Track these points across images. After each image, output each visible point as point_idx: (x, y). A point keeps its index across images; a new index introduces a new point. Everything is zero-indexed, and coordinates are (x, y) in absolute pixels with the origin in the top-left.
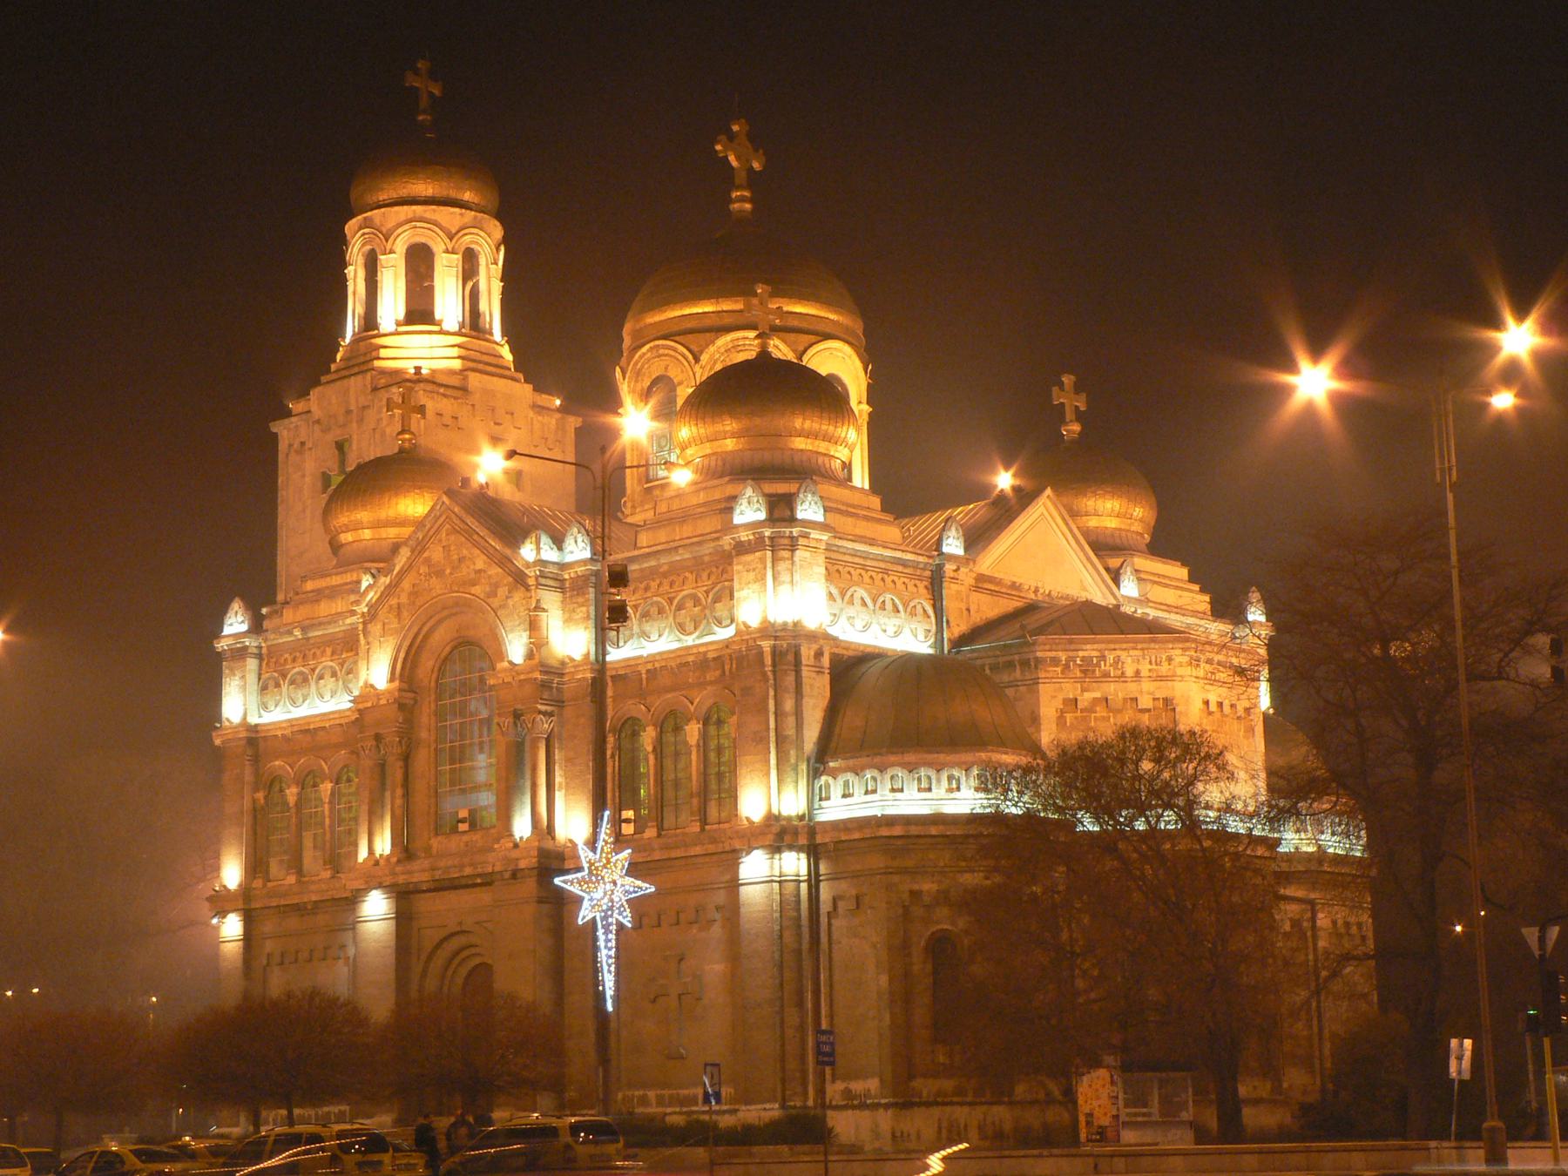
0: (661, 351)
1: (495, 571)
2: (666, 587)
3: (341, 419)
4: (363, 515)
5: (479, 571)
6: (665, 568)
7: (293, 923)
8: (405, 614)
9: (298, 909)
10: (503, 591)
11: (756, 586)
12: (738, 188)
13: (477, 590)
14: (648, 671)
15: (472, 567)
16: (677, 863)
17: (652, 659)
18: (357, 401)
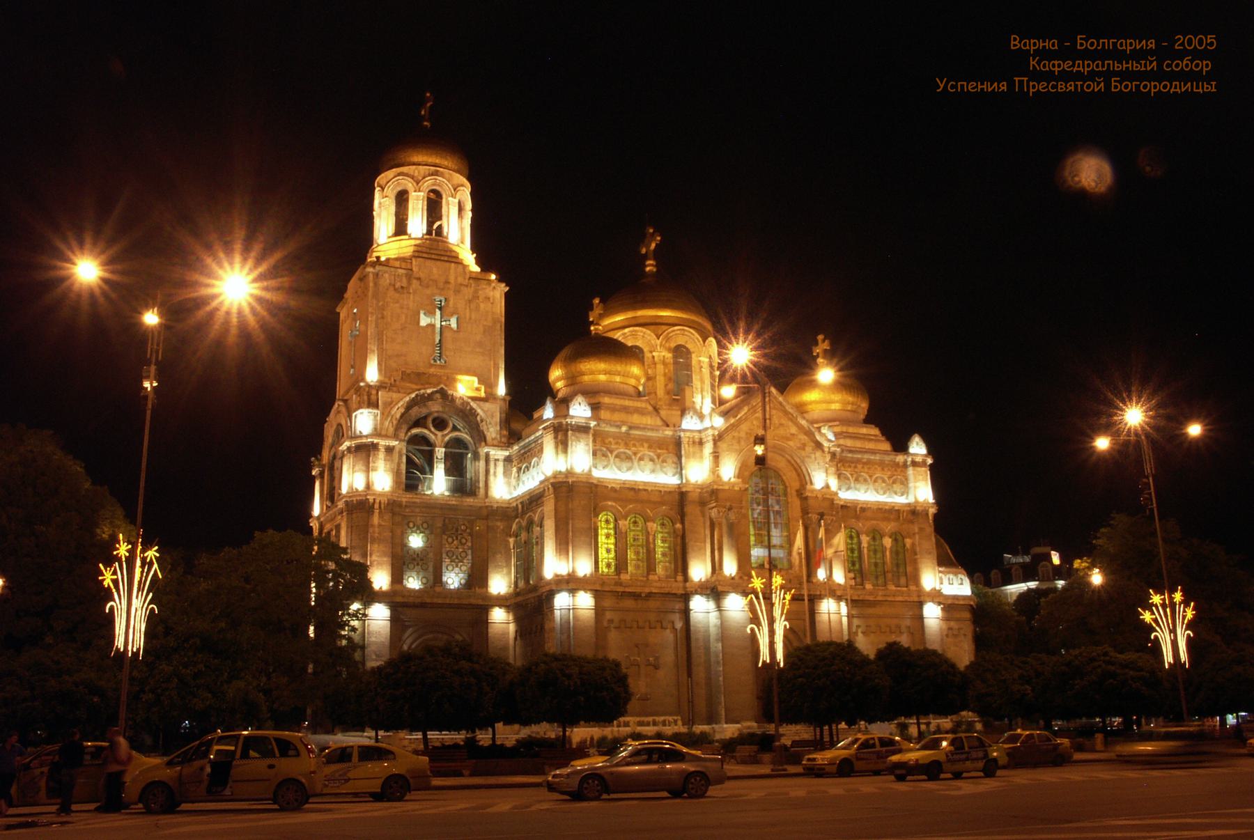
0: (686, 333)
1: (803, 437)
2: (866, 470)
3: (441, 285)
4: (602, 366)
5: (793, 435)
6: (865, 460)
7: (629, 603)
8: (743, 443)
9: (636, 596)
10: (808, 449)
11: (924, 482)
12: (650, 259)
13: (791, 443)
14: (861, 508)
15: (788, 431)
16: (887, 603)
17: (866, 503)
18: (456, 278)
